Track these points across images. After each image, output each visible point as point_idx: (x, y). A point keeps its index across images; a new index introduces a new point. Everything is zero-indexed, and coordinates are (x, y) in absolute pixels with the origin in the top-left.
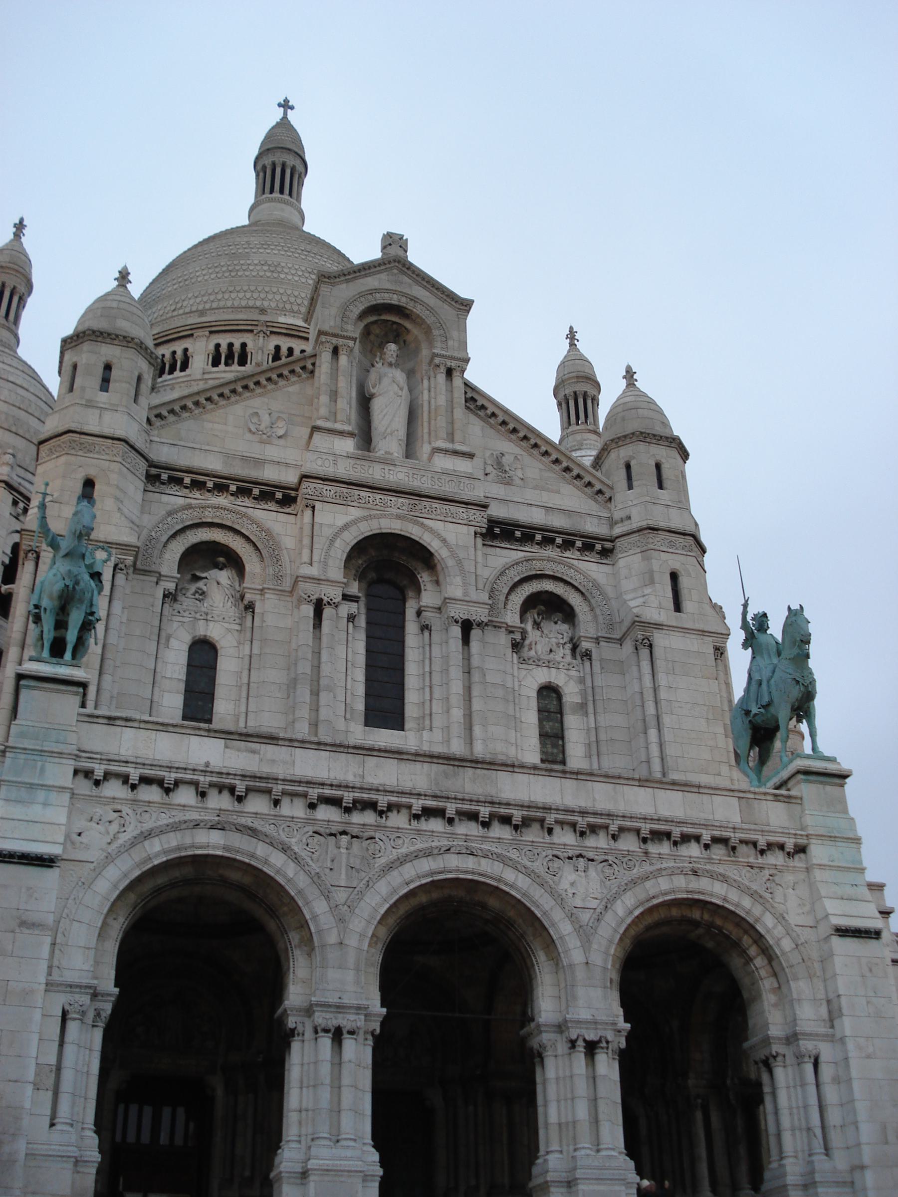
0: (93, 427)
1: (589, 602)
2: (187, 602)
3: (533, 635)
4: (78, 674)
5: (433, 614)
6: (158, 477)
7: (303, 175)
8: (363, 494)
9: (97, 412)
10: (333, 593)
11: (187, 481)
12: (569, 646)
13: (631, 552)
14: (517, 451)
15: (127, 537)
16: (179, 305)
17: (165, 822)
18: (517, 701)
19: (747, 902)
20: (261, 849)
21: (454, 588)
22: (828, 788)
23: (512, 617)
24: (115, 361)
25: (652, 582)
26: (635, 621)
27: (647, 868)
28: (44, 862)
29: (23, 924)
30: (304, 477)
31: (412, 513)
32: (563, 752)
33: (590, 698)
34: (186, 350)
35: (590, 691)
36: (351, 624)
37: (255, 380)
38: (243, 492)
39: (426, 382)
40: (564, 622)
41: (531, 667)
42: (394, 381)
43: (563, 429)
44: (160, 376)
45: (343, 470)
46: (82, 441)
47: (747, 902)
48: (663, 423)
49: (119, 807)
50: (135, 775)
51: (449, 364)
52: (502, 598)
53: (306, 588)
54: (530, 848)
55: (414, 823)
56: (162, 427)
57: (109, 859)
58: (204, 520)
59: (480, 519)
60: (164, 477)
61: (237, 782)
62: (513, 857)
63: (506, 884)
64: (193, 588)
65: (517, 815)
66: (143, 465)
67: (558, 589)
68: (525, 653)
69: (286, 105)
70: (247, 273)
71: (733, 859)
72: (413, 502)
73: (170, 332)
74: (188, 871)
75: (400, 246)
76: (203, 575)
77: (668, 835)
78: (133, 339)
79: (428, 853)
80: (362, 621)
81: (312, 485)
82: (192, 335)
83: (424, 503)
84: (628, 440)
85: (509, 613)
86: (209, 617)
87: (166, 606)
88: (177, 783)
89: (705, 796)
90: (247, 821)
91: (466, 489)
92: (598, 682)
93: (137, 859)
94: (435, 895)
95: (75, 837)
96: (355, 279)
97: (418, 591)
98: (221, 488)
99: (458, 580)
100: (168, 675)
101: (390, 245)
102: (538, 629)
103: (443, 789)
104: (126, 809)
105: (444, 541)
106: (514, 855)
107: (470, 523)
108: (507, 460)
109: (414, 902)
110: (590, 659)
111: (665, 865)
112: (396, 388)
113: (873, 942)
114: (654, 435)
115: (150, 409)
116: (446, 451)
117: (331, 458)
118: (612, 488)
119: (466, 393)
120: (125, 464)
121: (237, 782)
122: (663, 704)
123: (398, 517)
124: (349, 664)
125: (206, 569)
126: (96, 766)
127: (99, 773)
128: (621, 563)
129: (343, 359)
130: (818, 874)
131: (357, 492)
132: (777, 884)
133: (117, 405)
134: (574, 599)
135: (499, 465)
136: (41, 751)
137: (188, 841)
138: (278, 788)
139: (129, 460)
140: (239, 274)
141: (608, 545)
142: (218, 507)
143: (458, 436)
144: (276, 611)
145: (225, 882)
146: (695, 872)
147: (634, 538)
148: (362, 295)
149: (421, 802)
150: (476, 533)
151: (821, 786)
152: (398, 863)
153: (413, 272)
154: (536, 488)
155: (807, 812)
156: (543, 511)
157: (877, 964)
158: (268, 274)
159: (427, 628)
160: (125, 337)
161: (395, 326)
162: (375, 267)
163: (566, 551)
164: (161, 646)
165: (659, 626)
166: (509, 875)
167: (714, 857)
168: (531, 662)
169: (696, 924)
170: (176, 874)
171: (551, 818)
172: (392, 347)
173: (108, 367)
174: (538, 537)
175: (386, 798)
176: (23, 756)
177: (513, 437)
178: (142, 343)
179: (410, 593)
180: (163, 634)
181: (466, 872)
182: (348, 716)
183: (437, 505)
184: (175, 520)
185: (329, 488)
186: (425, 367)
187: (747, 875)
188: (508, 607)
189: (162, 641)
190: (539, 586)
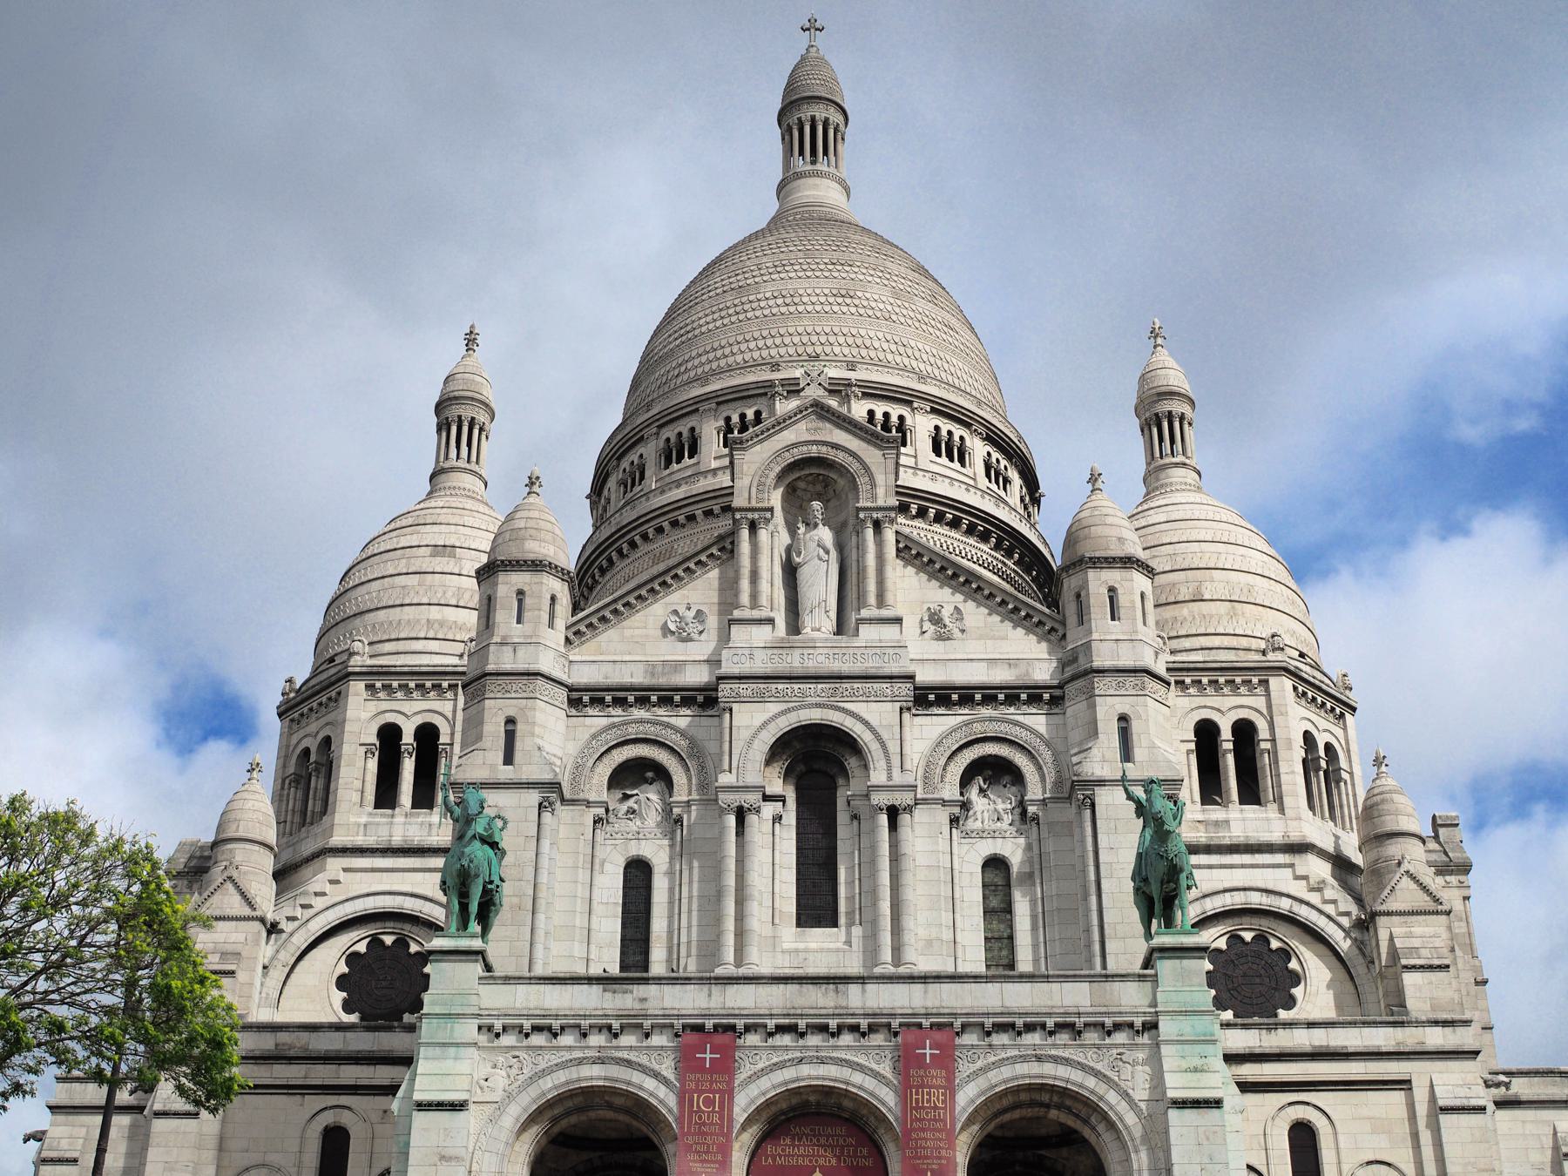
0: (508, 667)
1: (1036, 759)
2: (620, 825)
3: (979, 803)
4: (476, 944)
5: (862, 802)
6: (580, 699)
7: (842, 127)
8: (780, 686)
9: (509, 649)
10: (753, 798)
11: (608, 699)
12: (1017, 811)
13: (1078, 699)
14: (959, 597)
15: (547, 776)
16: (683, 369)
17: (555, 1062)
18: (956, 881)
19: (1091, 1082)
20: (636, 1077)
21: (878, 776)
22: (1186, 962)
23: (951, 791)
24: (526, 589)
25: (1096, 733)
26: (1073, 781)
27: (992, 1059)
28: (457, 1107)
29: (442, 1158)
30: (720, 678)
31: (832, 699)
32: (1011, 927)
33: (1037, 866)
34: (693, 429)
35: (1036, 859)
36: (777, 825)
37: (672, 573)
38: (665, 701)
39: (854, 538)
40: (1013, 785)
41: (974, 840)
42: (819, 545)
43: (1148, 464)
44: (667, 467)
45: (761, 664)
46: (499, 682)
47: (1091, 1082)
48: (1119, 539)
49: (517, 1053)
50: (527, 1024)
51: (875, 516)
52: (939, 771)
53: (725, 798)
54: (877, 1051)
55: (770, 1040)
56: (582, 643)
57: (509, 1097)
58: (628, 737)
59: (905, 689)
60: (586, 699)
61: (613, 1022)
62: (861, 1061)
63: (854, 1086)
64: (624, 807)
65: (864, 1023)
66: (562, 694)
67: (1002, 750)
68: (972, 824)
69: (812, 27)
70: (758, 313)
71: (1078, 1042)
72: (833, 686)
73: (669, 411)
74: (578, 1100)
75: (820, 384)
76: (635, 792)
77: (1013, 1026)
78: (541, 561)
79: (780, 1066)
80: (790, 818)
81: (728, 686)
82: (697, 410)
83: (844, 686)
84: (1078, 569)
85: (947, 786)
86: (641, 836)
87: (598, 831)
88: (562, 1028)
89: (1054, 984)
90: (624, 1055)
91: (891, 661)
92: (1050, 846)
93: (534, 1096)
94: (794, 1101)
95: (482, 1082)
96: (770, 436)
97: (847, 777)
98: (643, 701)
99: (882, 764)
100: (605, 901)
101: (808, 384)
102: (984, 796)
103: (797, 1006)
104: (522, 1054)
105: (866, 723)
106: (861, 1059)
107: (896, 699)
108: (946, 613)
109: (774, 1109)
110: (1038, 824)
111: (1009, 1055)
112: (821, 552)
113: (1213, 1114)
114: (1106, 559)
115: (567, 628)
116: (871, 621)
117: (747, 652)
118: (1064, 624)
119: (898, 542)
120: (542, 698)
121: (613, 1022)
122: (1102, 868)
123: (818, 705)
124: (777, 867)
125: (635, 785)
126: (496, 1022)
127: (498, 1025)
128: (1069, 712)
129: (763, 535)
130: (1165, 1050)
131: (774, 686)
132: (1124, 1062)
133: (531, 637)
134: (1020, 760)
135: (935, 618)
136: (450, 1014)
137: (575, 1076)
138: (647, 1023)
139: (547, 693)
140: (749, 315)
141: (1057, 692)
142: (641, 721)
143: (889, 598)
144: (703, 821)
145: (610, 1106)
146: (1039, 1059)
147: (1079, 683)
148: (778, 454)
149: (774, 1021)
150: (901, 709)
151: (1178, 961)
152: (755, 1077)
153: (833, 414)
154: (980, 638)
155: (1159, 989)
156: (984, 664)
157: (1215, 1132)
158: (783, 310)
159: (856, 818)
160: (533, 561)
161: (821, 477)
162: (790, 418)
163: (1010, 706)
164: (596, 873)
165: (1101, 782)
166: (857, 1078)
167: (1058, 1042)
168: (974, 835)
169: (1048, 1106)
170: (570, 1104)
171: (895, 1023)
172: (816, 505)
173: (520, 593)
174: (978, 697)
175: (743, 1021)
176: (435, 1021)
177: (953, 582)
178: (550, 563)
179: (841, 781)
180: (597, 861)
181: (817, 1078)
182: (777, 921)
183: (859, 685)
184: (599, 743)
185: (745, 686)
186: (852, 521)
187: (1095, 1056)
188: (946, 780)
189: (597, 867)
190: (981, 750)
